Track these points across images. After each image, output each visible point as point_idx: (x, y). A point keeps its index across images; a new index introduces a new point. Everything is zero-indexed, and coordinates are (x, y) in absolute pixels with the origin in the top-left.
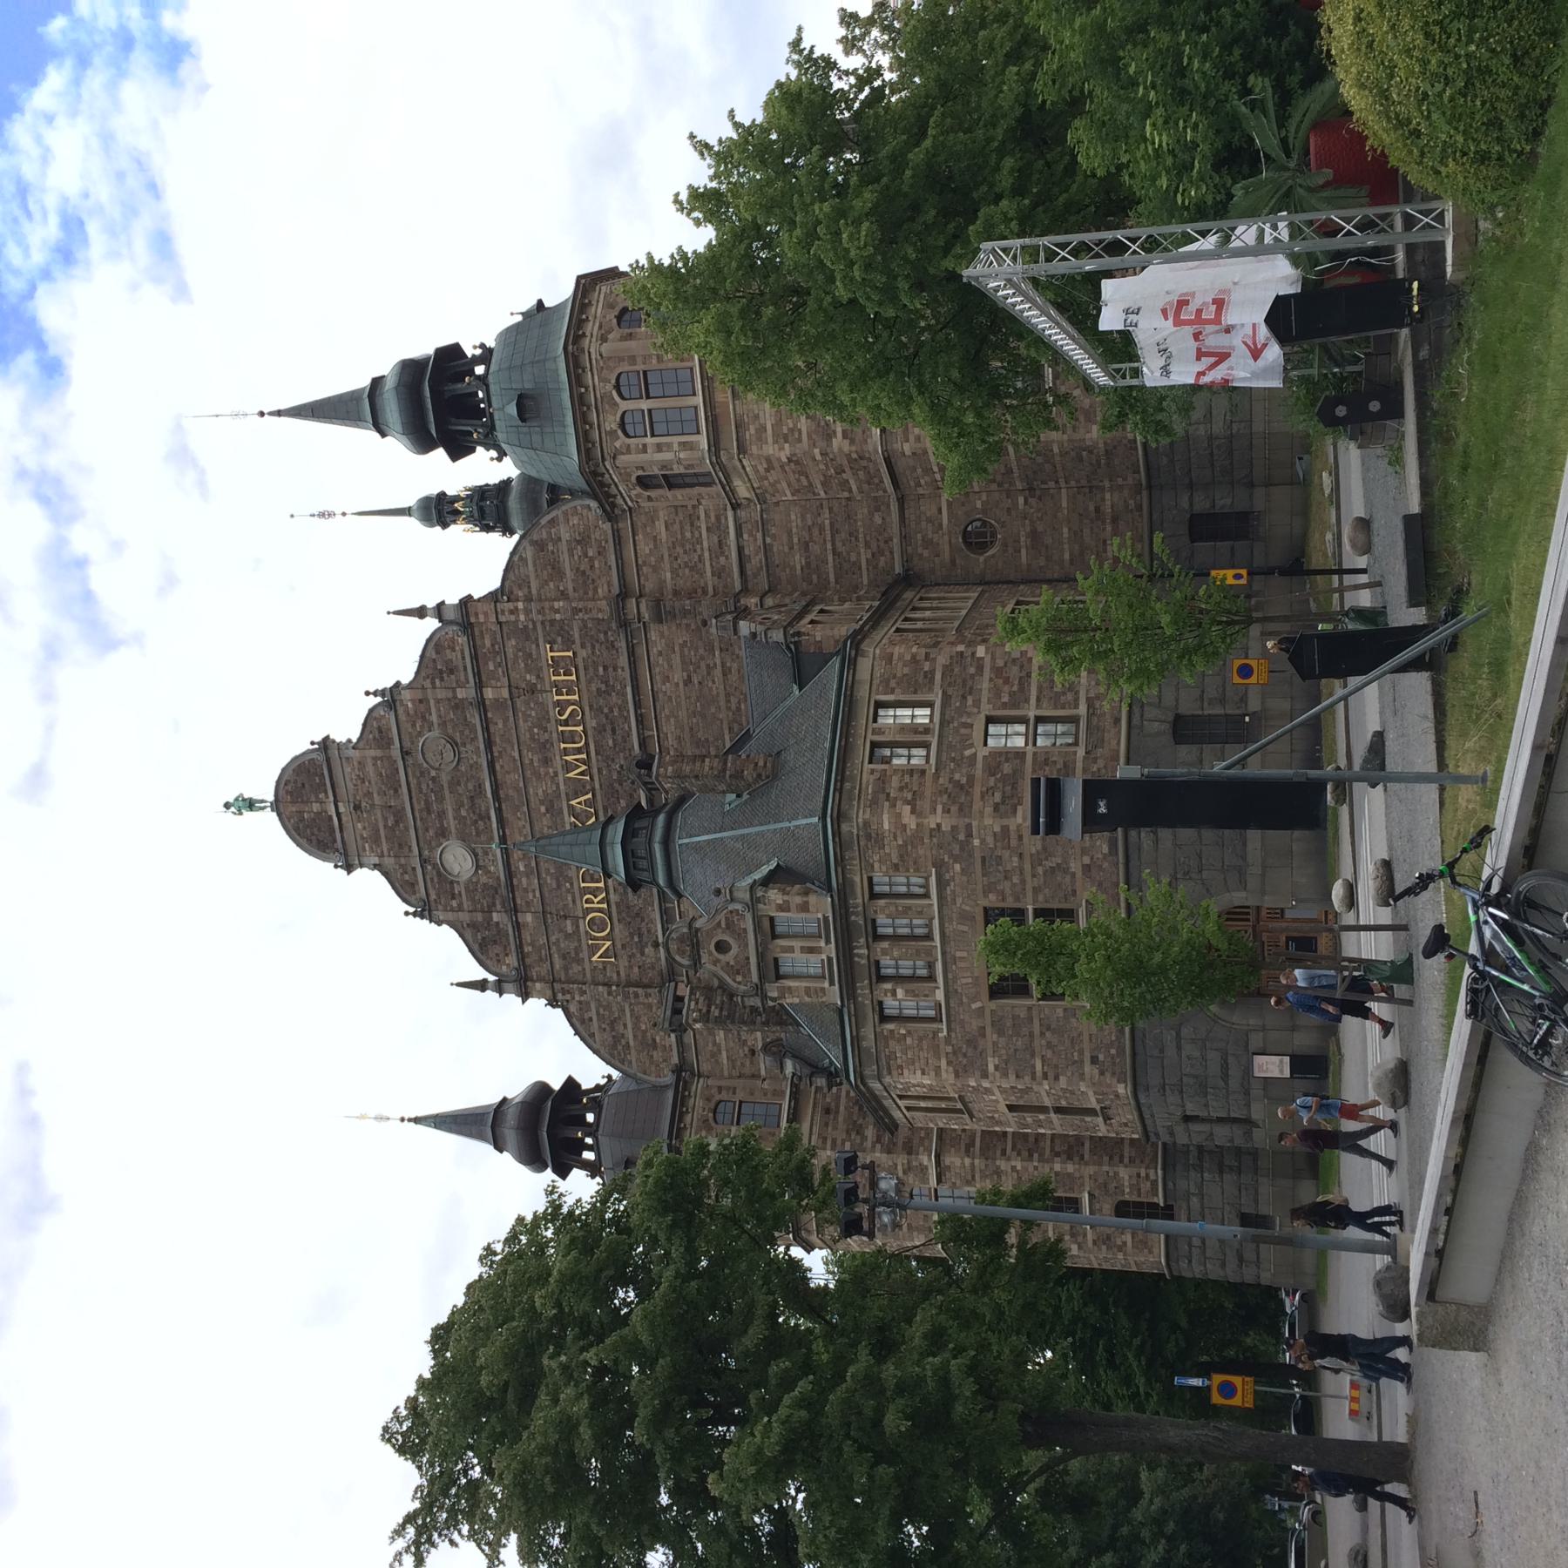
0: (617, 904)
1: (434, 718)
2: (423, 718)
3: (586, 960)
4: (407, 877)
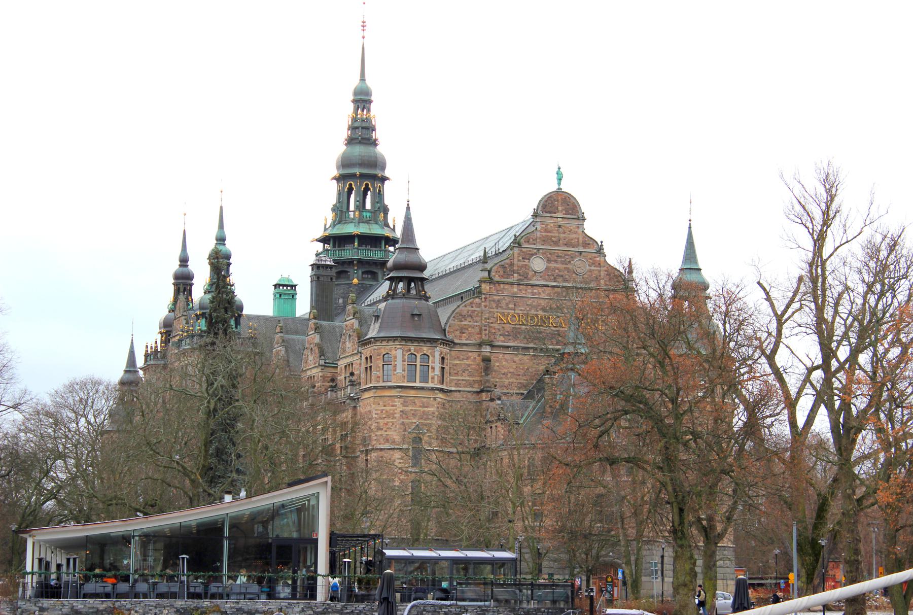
0: (520, 328)
1: (593, 268)
2: (593, 264)
3: (497, 310)
4: (531, 240)
